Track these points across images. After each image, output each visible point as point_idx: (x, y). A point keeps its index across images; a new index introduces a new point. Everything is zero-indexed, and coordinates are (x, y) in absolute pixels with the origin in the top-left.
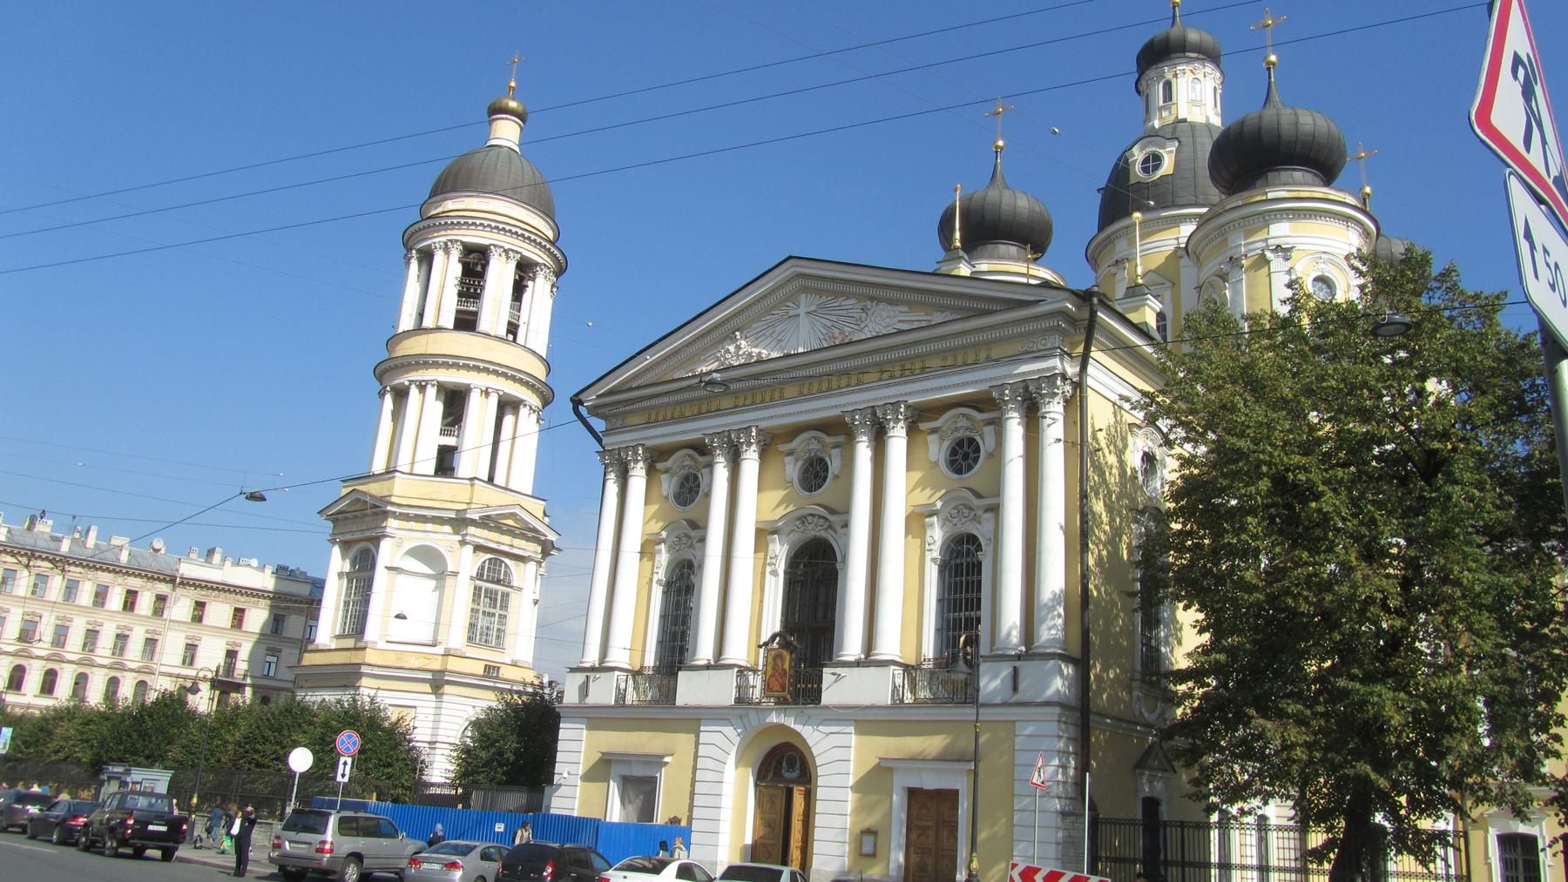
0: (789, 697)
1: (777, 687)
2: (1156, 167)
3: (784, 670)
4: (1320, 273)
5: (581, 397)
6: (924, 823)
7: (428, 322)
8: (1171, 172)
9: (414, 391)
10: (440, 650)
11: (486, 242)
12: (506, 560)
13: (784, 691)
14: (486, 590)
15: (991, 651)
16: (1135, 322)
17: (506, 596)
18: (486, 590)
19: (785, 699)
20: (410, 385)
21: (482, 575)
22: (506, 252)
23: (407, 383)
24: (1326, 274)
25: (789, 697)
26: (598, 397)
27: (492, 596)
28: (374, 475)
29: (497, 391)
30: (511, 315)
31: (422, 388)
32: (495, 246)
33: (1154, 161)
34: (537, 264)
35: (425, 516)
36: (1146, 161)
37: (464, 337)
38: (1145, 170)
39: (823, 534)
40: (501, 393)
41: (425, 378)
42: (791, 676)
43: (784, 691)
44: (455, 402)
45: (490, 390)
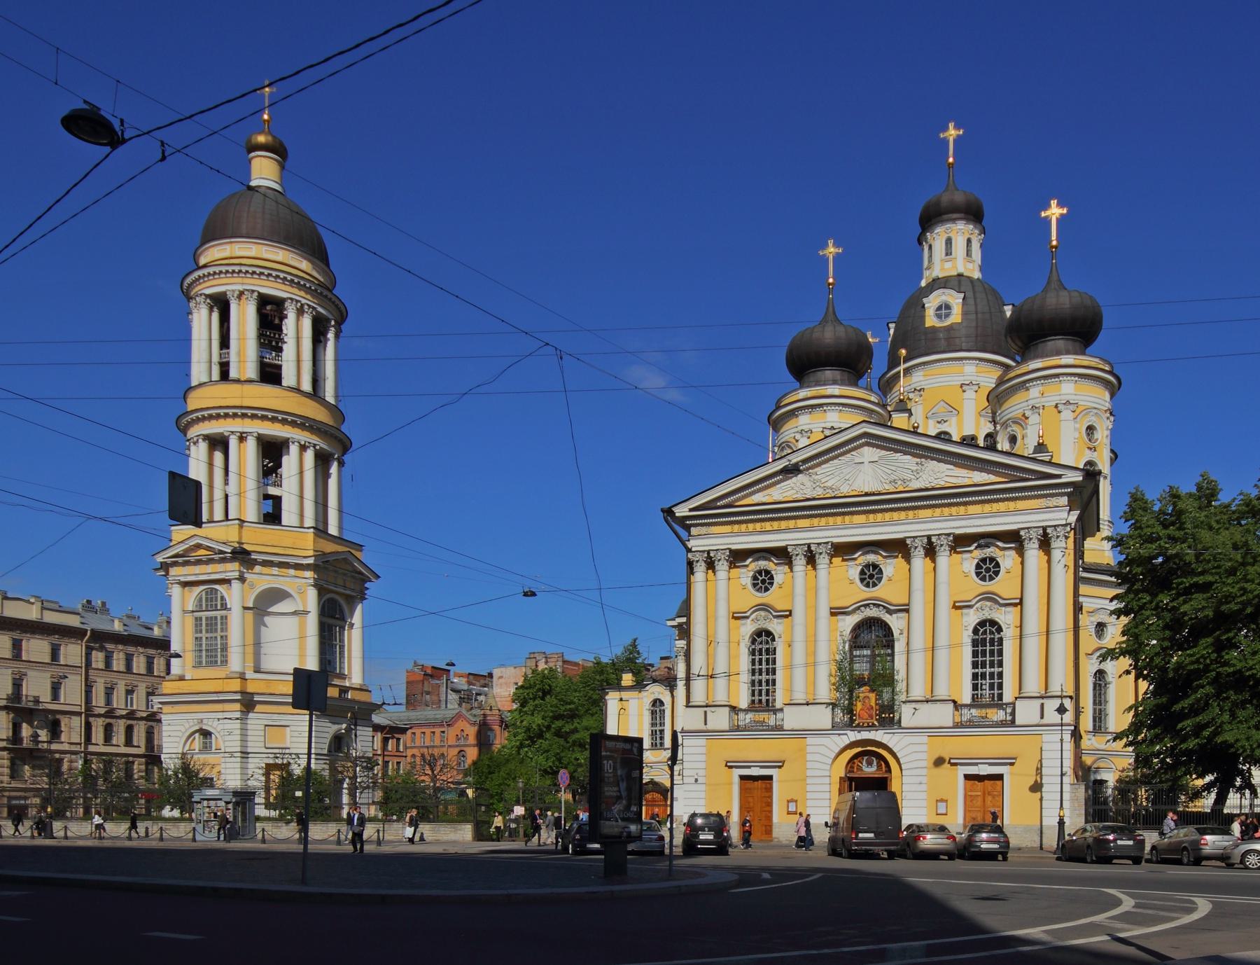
0: (876, 723)
1: (866, 716)
2: (947, 316)
3: (870, 706)
4: (1090, 423)
5: (673, 509)
6: (974, 794)
8: (960, 321)
12: (217, 587)
13: (872, 719)
15: (1046, 693)
16: (933, 435)
19: (873, 724)
20: (229, 435)
23: (227, 434)
24: (1094, 424)
25: (876, 723)
26: (691, 510)
31: (242, 438)
33: (944, 309)
35: (272, 561)
36: (939, 308)
38: (939, 317)
39: (882, 616)
41: (245, 430)
42: (876, 710)
43: (872, 719)
44: (272, 452)
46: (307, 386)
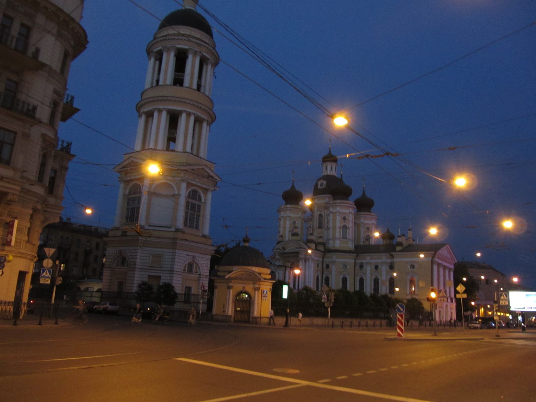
7: (161, 83)
9: (156, 114)
10: (173, 229)
11: (187, 47)
14: (191, 203)
17: (199, 206)
18: (191, 203)
21: (190, 196)
22: (196, 52)
27: (193, 205)
28: (137, 152)
29: (194, 114)
30: (198, 81)
31: (160, 111)
32: (191, 49)
34: (208, 59)
37: (178, 88)
40: (196, 115)
45: (191, 114)
46: (195, 87)
